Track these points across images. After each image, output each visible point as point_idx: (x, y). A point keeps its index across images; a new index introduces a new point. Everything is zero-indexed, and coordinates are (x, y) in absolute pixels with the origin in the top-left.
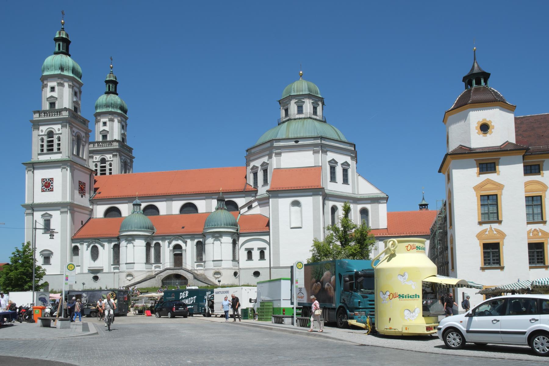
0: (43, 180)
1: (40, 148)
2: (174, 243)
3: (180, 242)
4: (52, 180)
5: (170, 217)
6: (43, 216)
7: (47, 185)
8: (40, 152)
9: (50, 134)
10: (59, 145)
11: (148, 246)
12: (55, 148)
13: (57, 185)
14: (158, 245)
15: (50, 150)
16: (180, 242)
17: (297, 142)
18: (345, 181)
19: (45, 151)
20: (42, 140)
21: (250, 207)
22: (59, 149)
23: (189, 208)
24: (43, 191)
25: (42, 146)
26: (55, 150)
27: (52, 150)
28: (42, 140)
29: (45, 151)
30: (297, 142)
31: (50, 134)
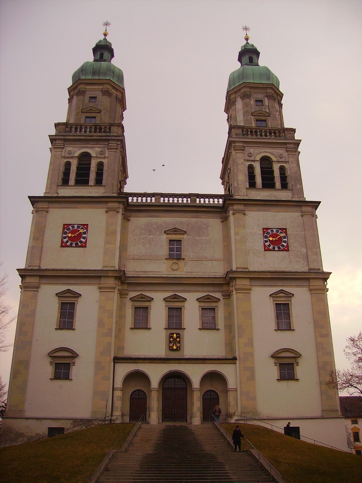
0: (66, 227)
1: (61, 176)
8: (60, 182)
9: (85, 158)
12: (92, 176)
13: (95, 237)
15: (82, 180)
19: (72, 181)
20: (68, 165)
22: (99, 182)
24: (63, 245)
26: (92, 182)
28: (68, 165)
29: (72, 181)
31: (85, 158)
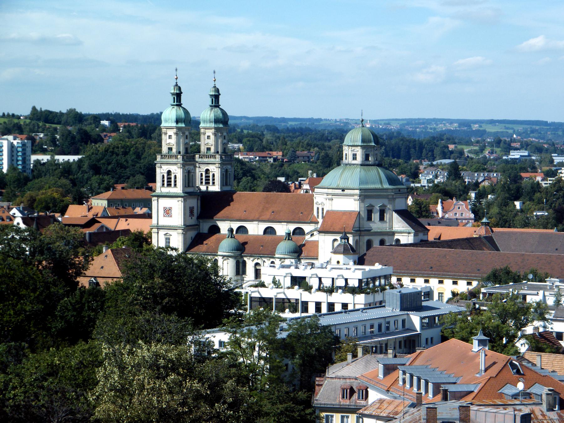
2: (256, 261)
3: (259, 261)
4: (170, 209)
5: (256, 237)
6: (165, 234)
7: (168, 212)
10: (175, 181)
11: (238, 264)
12: (173, 183)
14: (244, 263)
15: (169, 185)
16: (259, 261)
17: (343, 190)
18: (382, 218)
19: (166, 185)
21: (312, 235)
23: (269, 231)
25: (163, 181)
27: (171, 185)
29: (166, 185)
30: (343, 190)
